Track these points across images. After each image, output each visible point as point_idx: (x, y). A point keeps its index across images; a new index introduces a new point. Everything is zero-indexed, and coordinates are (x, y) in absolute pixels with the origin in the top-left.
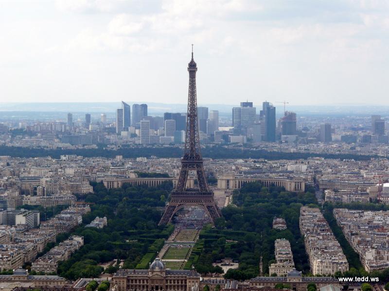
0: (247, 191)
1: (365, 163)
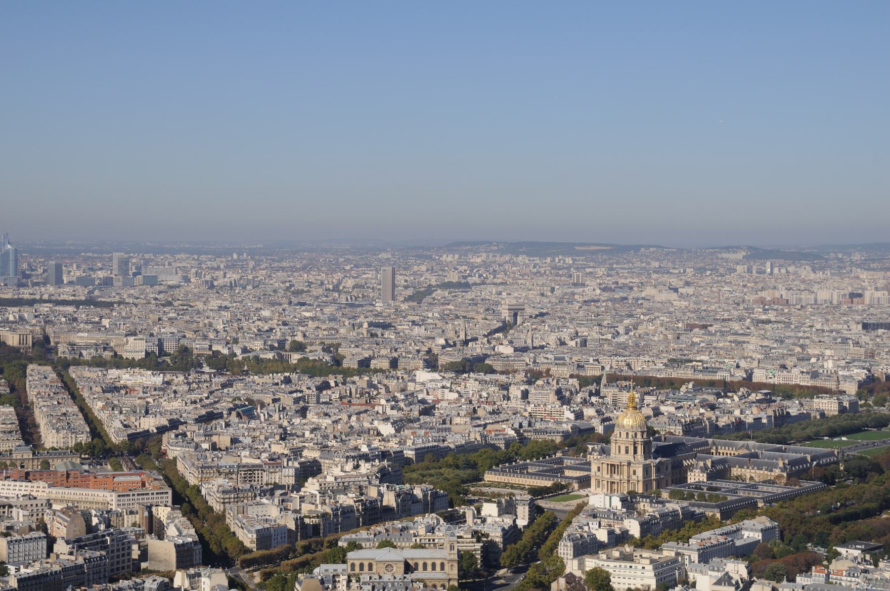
1: (106, 311)
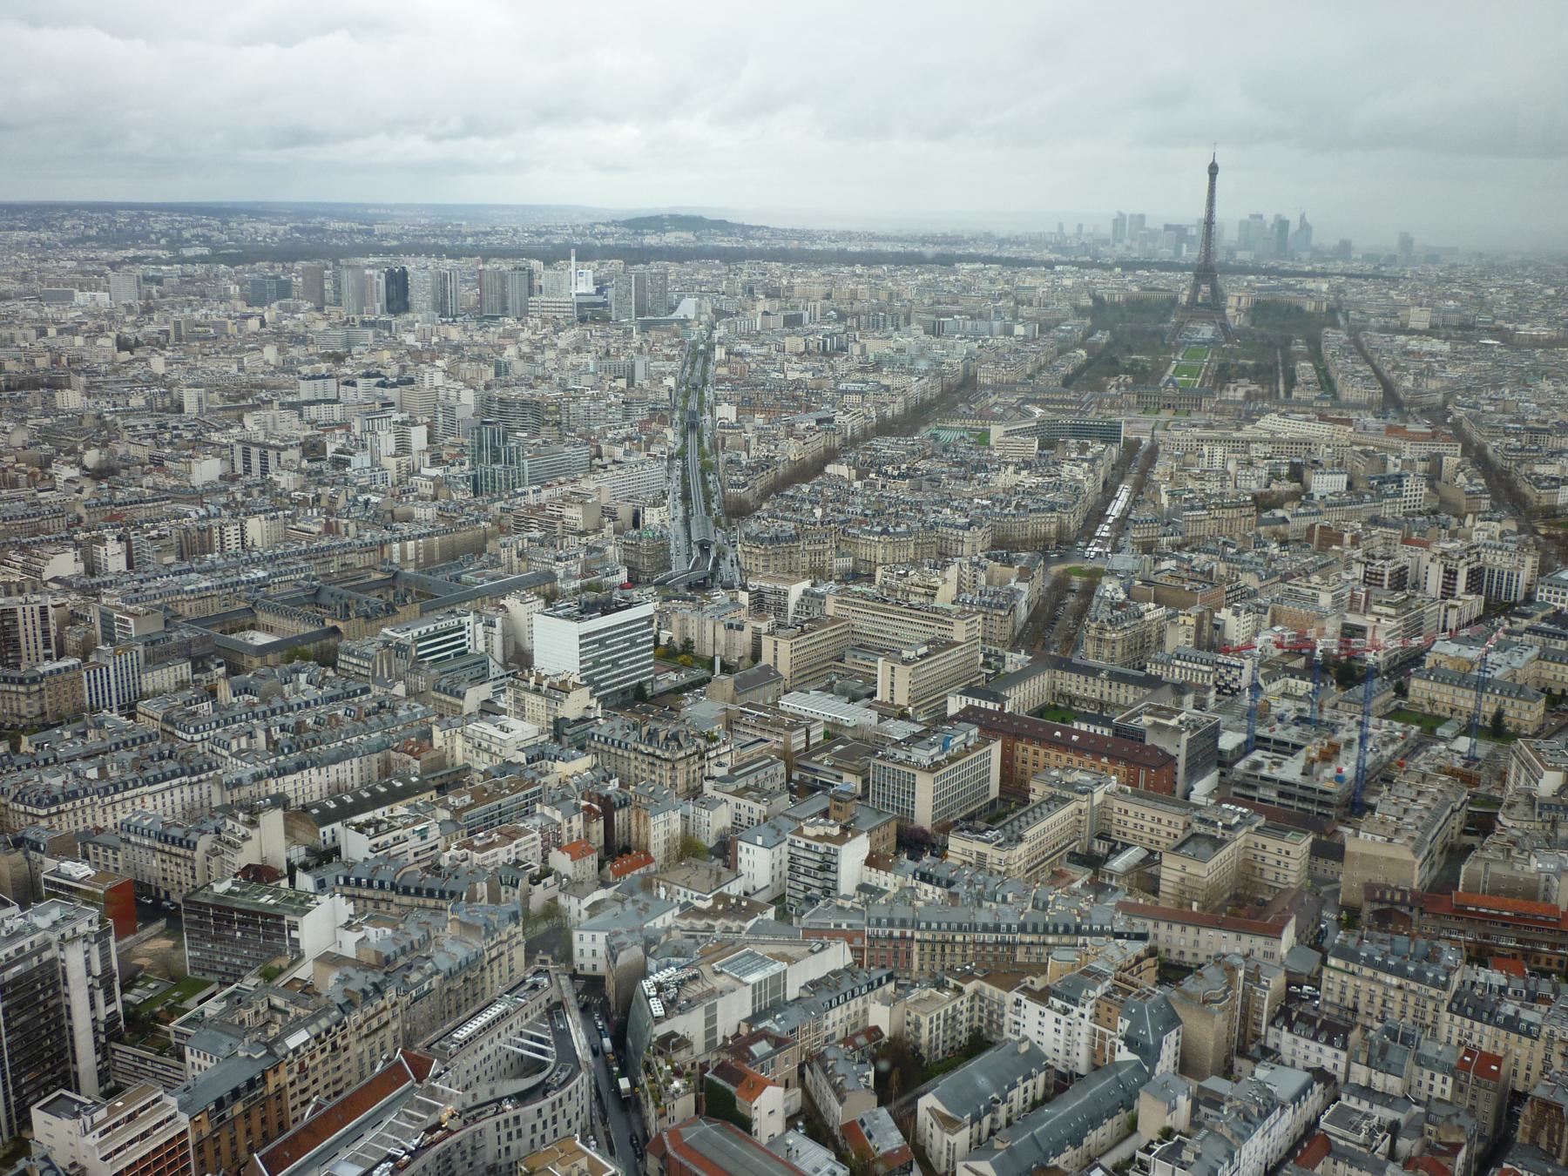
0: (1260, 310)
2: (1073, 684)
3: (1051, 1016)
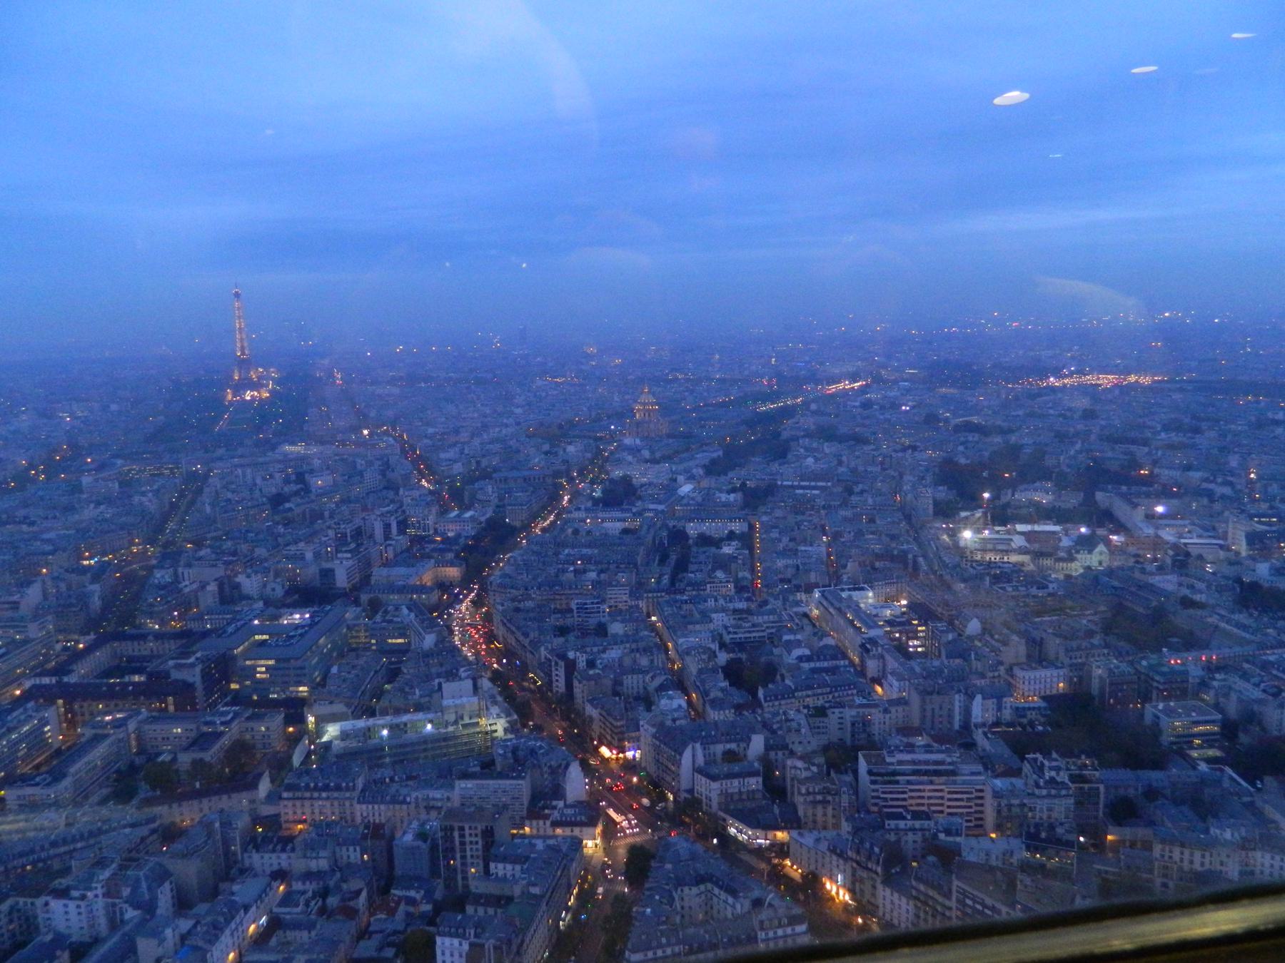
2: (129, 648)
3: (72, 905)
